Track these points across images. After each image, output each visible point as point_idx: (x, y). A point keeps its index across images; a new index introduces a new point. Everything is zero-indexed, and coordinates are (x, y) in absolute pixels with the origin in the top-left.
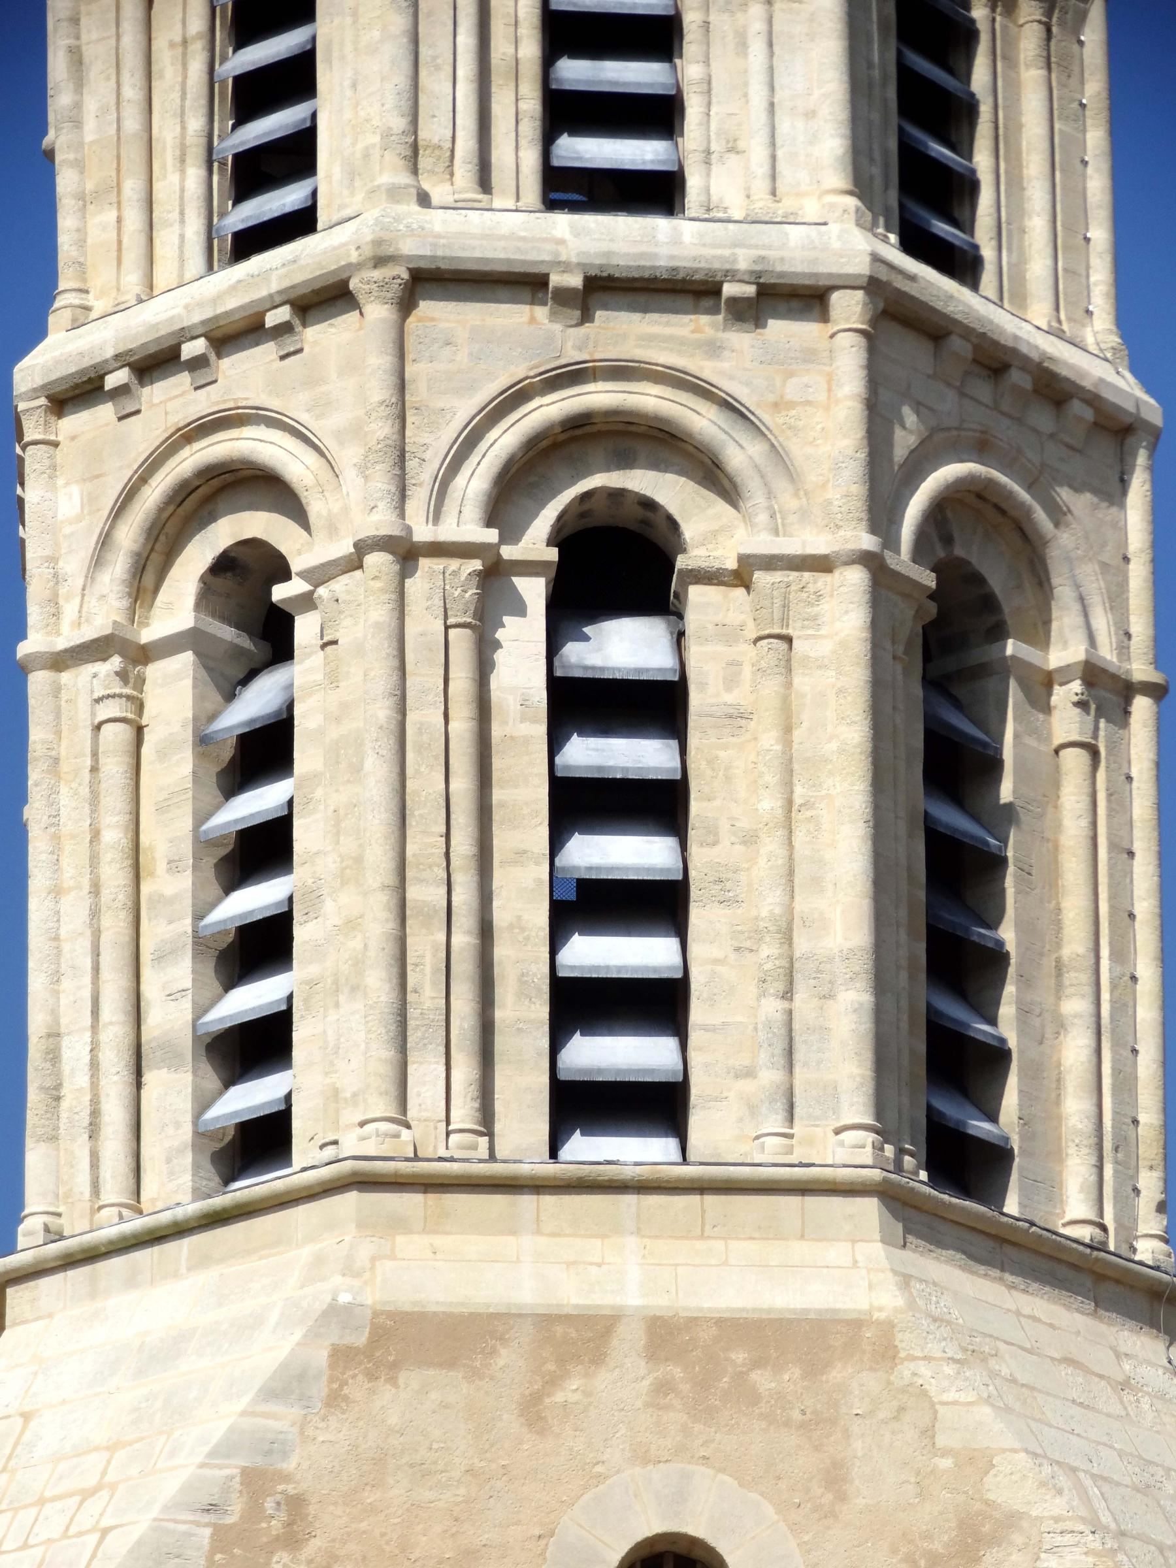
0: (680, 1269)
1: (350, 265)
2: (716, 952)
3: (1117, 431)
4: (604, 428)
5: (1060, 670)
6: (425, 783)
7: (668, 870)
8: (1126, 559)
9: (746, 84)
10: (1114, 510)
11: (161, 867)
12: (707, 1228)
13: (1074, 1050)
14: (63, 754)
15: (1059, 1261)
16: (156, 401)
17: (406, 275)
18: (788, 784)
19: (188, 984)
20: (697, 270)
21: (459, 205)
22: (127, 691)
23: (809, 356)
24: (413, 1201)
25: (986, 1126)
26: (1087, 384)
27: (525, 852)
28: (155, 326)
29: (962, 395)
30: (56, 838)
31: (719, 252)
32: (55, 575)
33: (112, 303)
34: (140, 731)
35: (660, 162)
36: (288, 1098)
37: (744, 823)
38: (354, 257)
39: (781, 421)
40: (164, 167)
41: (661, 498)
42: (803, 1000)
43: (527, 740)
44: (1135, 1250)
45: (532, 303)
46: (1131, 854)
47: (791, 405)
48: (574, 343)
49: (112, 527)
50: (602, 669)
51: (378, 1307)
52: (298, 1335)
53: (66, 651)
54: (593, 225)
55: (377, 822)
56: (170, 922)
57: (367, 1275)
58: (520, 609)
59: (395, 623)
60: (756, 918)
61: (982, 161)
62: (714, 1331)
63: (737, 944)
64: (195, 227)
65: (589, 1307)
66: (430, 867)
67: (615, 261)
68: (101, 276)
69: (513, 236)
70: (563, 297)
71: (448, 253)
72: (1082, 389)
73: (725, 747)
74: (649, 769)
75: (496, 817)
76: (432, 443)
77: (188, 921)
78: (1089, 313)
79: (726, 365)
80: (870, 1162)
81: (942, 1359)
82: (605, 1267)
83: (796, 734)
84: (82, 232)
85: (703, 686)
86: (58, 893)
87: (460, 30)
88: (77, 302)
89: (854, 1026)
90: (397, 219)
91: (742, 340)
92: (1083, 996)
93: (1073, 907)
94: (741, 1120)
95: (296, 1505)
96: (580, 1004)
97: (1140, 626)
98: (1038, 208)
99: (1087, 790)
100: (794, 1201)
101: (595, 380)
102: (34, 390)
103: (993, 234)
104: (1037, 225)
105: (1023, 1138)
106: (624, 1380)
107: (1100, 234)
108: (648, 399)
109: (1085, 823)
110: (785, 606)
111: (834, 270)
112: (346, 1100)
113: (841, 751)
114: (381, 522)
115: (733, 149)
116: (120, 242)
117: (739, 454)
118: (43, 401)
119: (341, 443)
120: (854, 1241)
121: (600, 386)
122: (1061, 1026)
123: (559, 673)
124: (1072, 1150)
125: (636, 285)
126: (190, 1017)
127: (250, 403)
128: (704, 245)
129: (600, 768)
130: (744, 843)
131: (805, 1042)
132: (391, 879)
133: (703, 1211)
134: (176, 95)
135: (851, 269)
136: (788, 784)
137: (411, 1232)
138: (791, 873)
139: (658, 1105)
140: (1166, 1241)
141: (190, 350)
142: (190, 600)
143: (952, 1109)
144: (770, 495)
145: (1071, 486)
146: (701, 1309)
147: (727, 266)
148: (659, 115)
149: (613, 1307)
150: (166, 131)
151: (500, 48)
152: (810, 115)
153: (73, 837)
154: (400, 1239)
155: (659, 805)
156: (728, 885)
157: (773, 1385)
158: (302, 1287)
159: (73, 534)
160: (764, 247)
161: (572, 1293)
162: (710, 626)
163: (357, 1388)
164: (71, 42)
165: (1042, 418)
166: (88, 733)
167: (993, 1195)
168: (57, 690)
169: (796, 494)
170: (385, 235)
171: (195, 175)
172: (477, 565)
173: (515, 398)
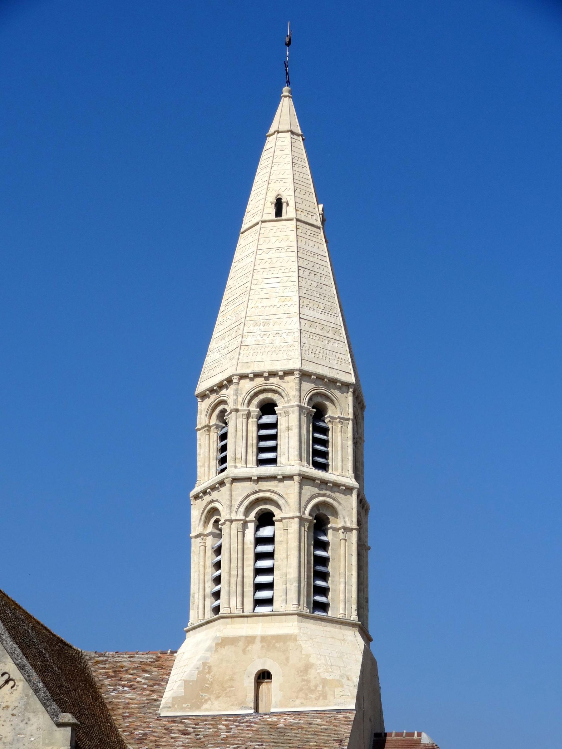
23: (291, 486)
42: (288, 586)
48: (256, 487)
64: (214, 470)
76: (236, 504)
91: (281, 484)
95: (210, 667)
104: (340, 457)
106: (257, 646)
108: (267, 495)
117: (281, 502)
139: (269, 602)
161: (250, 633)
168: (195, 541)
171: (215, 462)
173: (248, 496)
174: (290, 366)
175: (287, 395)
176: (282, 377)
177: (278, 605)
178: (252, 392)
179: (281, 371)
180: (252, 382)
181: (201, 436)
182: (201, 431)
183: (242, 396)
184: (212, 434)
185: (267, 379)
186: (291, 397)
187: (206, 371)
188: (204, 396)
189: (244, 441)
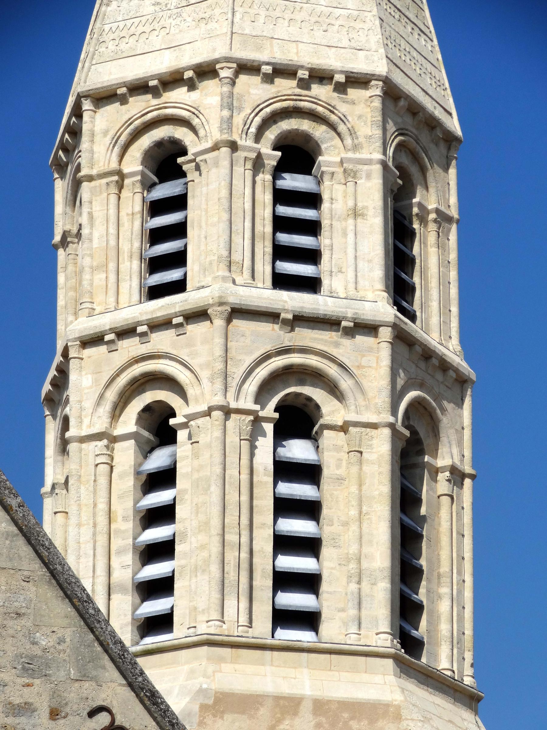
0: (323, 682)
1: (209, 304)
2: (332, 565)
3: (462, 382)
4: (295, 370)
5: (441, 467)
6: (232, 497)
7: (316, 534)
8: (463, 428)
9: (346, 248)
10: (460, 409)
11: (120, 519)
12: (332, 667)
13: (444, 606)
14: (82, 474)
15: (444, 684)
16: (124, 346)
17: (230, 310)
18: (360, 506)
19: (131, 563)
20: (333, 316)
21: (246, 285)
22: (109, 453)
23: (370, 350)
24: (227, 651)
25: (415, 632)
26: (455, 364)
27: (265, 524)
28: (127, 320)
29: (417, 366)
30: (79, 505)
31: (341, 310)
32: (81, 407)
33: (104, 308)
34: (112, 467)
35: (314, 274)
36: (172, 608)
37: (343, 518)
38: (211, 302)
39: (360, 373)
40: (124, 259)
41: (315, 397)
42: (365, 585)
43: (266, 483)
44: (463, 681)
45: (273, 323)
46: (463, 536)
47: (364, 367)
48: (288, 338)
49: (104, 392)
50: (293, 458)
51: (217, 690)
52: (188, 699)
53: (86, 436)
54: (296, 296)
55: (216, 510)
56: (123, 540)
57: (212, 678)
58: (264, 435)
59: (223, 438)
60: (347, 554)
61: (416, 279)
62: (337, 705)
63: (339, 563)
64: (135, 283)
65: (293, 694)
66: (233, 528)
67: (304, 310)
68: (99, 298)
69: (268, 298)
70: (285, 322)
71: (245, 303)
72: (453, 366)
73: (336, 490)
74: (309, 496)
75: (254, 511)
77: (131, 540)
78: (450, 337)
79: (341, 351)
80: (390, 646)
81: (418, 720)
82: (297, 679)
83: (364, 488)
84: (92, 280)
85: (329, 467)
86: (80, 526)
87: (246, 220)
88: (90, 306)
89: (384, 596)
90: (227, 289)
91: (347, 342)
92: (448, 587)
93: (444, 554)
94: (340, 627)
96: (283, 581)
97: (468, 453)
98: (435, 299)
99: (450, 512)
100: (363, 658)
101: (294, 353)
102: (75, 338)
103: (420, 307)
104: (434, 305)
105: (427, 638)
107: (455, 309)
108: (313, 361)
109: (449, 524)
110: (360, 440)
111: (382, 319)
112: (199, 612)
113: (380, 495)
114: (218, 400)
115: (340, 271)
116: (107, 286)
118: (78, 343)
119: (201, 369)
120: (384, 675)
121: (296, 355)
122: (440, 597)
123: (277, 459)
124: (443, 643)
125: (311, 319)
126: (131, 576)
127: (164, 351)
128: (336, 307)
129: (291, 495)
130: (342, 526)
131: (366, 600)
132: (220, 532)
133: (331, 661)
134: (130, 234)
135: (387, 320)
136: (360, 506)
137: (227, 663)
138: (361, 538)
139: (309, 620)
140: (473, 678)
141: (140, 329)
142: (134, 421)
143: (407, 627)
144: (355, 399)
145: (447, 401)
146: (332, 697)
147: (344, 315)
148: (312, 256)
149: (301, 695)
150: (125, 246)
151: (259, 228)
152: (370, 261)
153: (86, 505)
154: (223, 665)
155: (311, 509)
156: (337, 541)
157: (358, 726)
158: (187, 680)
159: (88, 393)
160: (357, 309)
161: (286, 688)
162: (331, 445)
163: (209, 720)
164: (89, 210)
165: (439, 376)
166: (93, 467)
167: (418, 657)
168: (81, 450)
169: (365, 400)
170: (223, 295)
171: (136, 263)
172: (251, 418)
173: (266, 357)
174: (360, 65)
175: (352, 132)
176: (341, 88)
177: (331, 630)
179: (342, 72)
180: (267, 86)
181: (93, 192)
182: (93, 183)
183: (243, 115)
184: (125, 193)
185: (304, 84)
186: (361, 140)
188: (104, 97)
189: (248, 224)
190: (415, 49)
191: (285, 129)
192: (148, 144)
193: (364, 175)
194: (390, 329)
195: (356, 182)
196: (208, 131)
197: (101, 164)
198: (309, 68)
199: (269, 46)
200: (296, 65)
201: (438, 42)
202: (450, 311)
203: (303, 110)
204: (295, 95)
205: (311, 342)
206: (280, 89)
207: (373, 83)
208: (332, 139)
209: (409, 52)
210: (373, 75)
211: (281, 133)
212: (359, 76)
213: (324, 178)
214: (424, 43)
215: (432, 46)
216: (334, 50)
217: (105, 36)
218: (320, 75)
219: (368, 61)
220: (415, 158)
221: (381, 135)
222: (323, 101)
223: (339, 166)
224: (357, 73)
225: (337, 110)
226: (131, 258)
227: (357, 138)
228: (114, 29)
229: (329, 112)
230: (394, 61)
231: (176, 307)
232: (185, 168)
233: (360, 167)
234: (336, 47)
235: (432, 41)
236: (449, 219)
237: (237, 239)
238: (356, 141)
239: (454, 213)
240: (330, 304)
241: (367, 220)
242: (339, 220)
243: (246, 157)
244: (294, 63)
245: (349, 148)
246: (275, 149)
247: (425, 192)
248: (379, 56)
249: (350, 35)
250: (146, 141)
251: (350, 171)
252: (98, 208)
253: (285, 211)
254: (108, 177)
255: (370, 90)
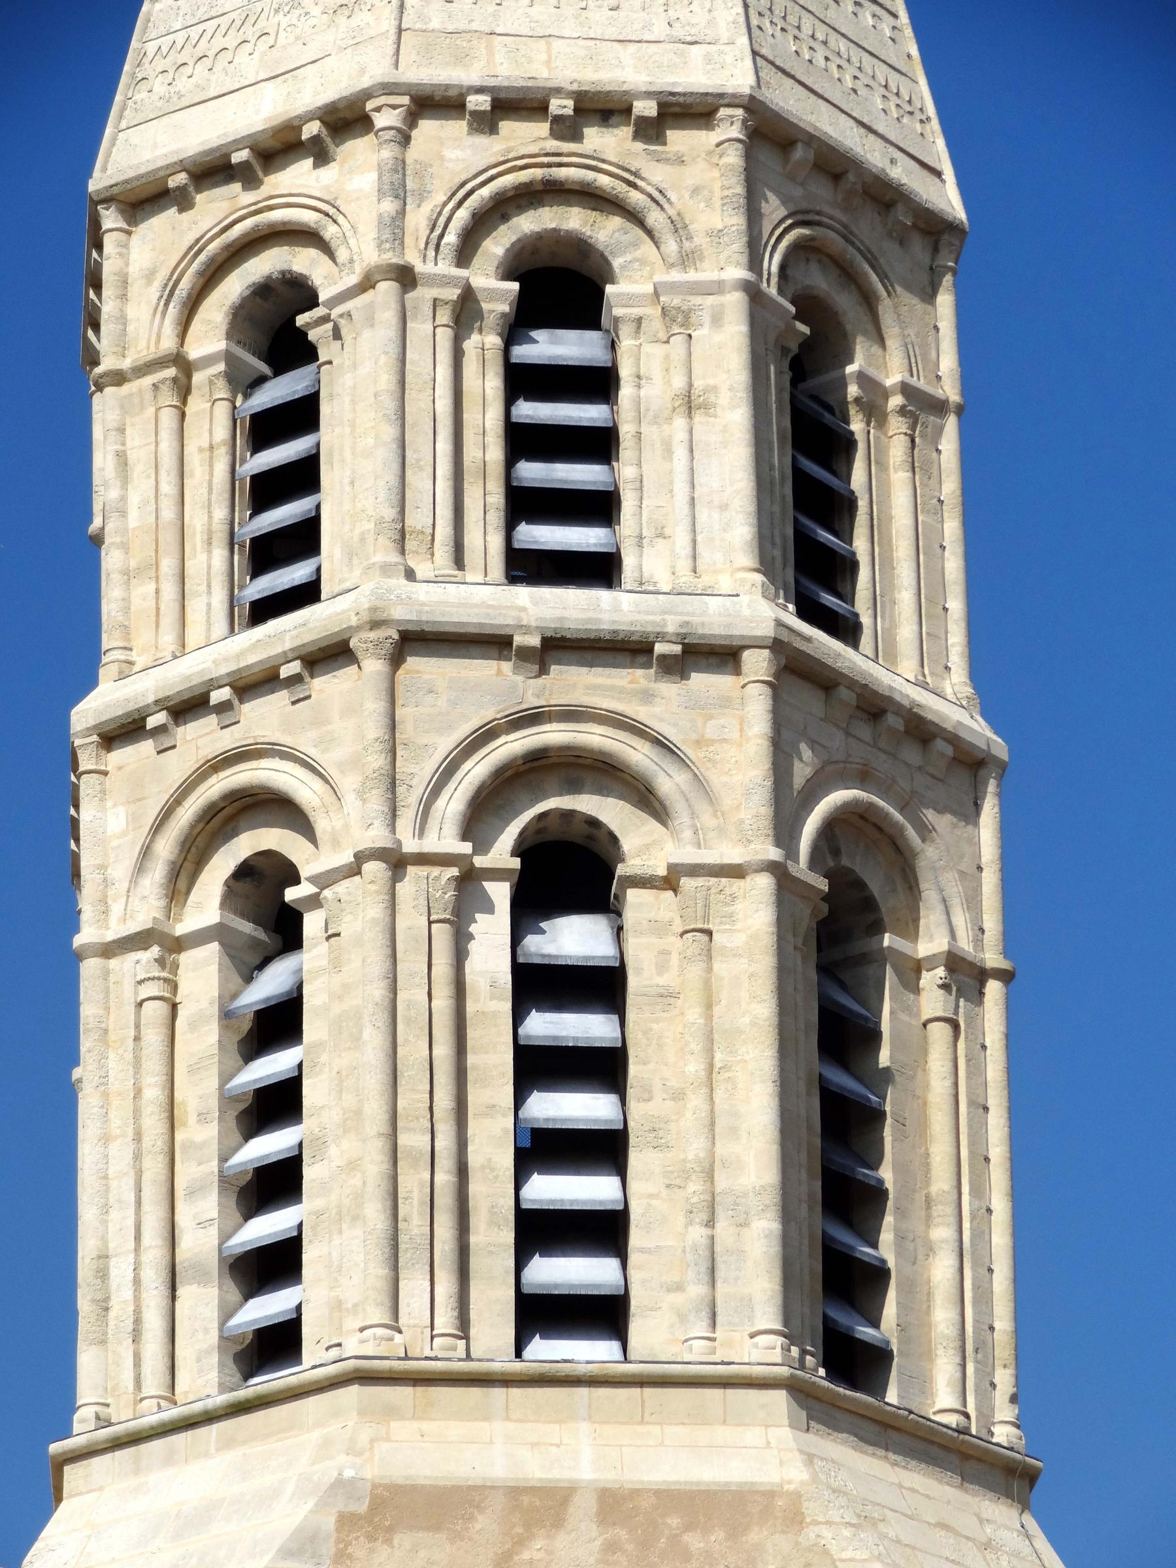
0: (624, 1449)
1: (350, 628)
2: (650, 1188)
3: (971, 764)
4: (556, 760)
5: (927, 958)
6: (413, 1050)
7: (611, 1121)
8: (980, 869)
9: (671, 482)
10: (970, 827)
11: (192, 1119)
12: (646, 1415)
13: (941, 1269)
14: (111, 1027)
15: (932, 1443)
16: (188, 738)
17: (396, 636)
18: (710, 1051)
19: (216, 1215)
20: (633, 633)
21: (439, 579)
22: (165, 974)
23: (725, 702)
24: (403, 1394)
25: (870, 1331)
26: (948, 726)
27: (494, 1106)
28: (188, 678)
29: (848, 734)
30: (106, 1095)
31: (651, 618)
32: (105, 880)
33: (151, 658)
34: (174, 1007)
35: (601, 545)
36: (299, 1308)
37: (673, 1083)
38: (354, 621)
39: (702, 755)
40: (194, 548)
41: (603, 818)
42: (723, 1228)
43: (495, 1015)
44: (992, 1434)
45: (499, 659)
46: (986, 1109)
47: (711, 742)
48: (533, 691)
49: (152, 841)
50: (557, 957)
51: (377, 1481)
52: (310, 1504)
53: (114, 941)
54: (548, 596)
55: (374, 1081)
56: (200, 1164)
57: (367, 1454)
58: (489, 908)
59: (388, 919)
60: (684, 1160)
61: (860, 545)
62: (653, 1500)
63: (667, 1182)
64: (219, 597)
65: (550, 1480)
66: (417, 1118)
68: (142, 638)
69: (484, 604)
70: (525, 654)
71: (431, 618)
73: (657, 1021)
74: (595, 1039)
75: (471, 1076)
76: (418, 772)
77: (215, 1163)
78: (947, 668)
79: (657, 710)
80: (779, 1361)
81: (842, 1523)
82: (562, 1447)
83: (717, 1010)
84: (126, 600)
85: (639, 971)
86: (107, 1140)
87: (438, 438)
88: (123, 658)
89: (765, 1249)
90: (390, 591)
91: (670, 690)
92: (948, 1225)
93: (940, 1151)
94: (672, 1326)
96: (539, 1231)
97: (992, 922)
99: (950, 1056)
100: (716, 1393)
101: (550, 722)
102: (88, 729)
103: (870, 604)
104: (905, 598)
105: (899, 1343)
107: (956, 605)
108: (594, 737)
109: (948, 1083)
110: (707, 906)
112: (348, 1309)
113: (753, 1024)
114: (376, 836)
115: (661, 535)
116: (158, 609)
117: (668, 782)
118: (95, 738)
119: (342, 772)
120: (767, 1426)
121: (555, 726)
122: (930, 1250)
123: (521, 960)
124: (940, 1352)
125: (583, 645)
126: (216, 1242)
129: (555, 1038)
130: (673, 1099)
131: (725, 1262)
132: (385, 1128)
133: (643, 1401)
134: (205, 491)
135: (759, 633)
136: (710, 1051)
137: (403, 1419)
138: (713, 1124)
139: (605, 1314)
140: (1018, 1427)
141: (217, 696)
142: (216, 901)
143: (843, 1317)
144: (693, 815)
145: (935, 809)
146: (642, 1482)
147: (658, 630)
148: (600, 507)
149: (569, 1481)
150: (196, 520)
151: (471, 453)
152: (724, 507)
153: (120, 1094)
154: (394, 1425)
155: (604, 1068)
156: (661, 1133)
157: (702, 1545)
158: (313, 1464)
159: (119, 847)
160: (688, 614)
161: (536, 1469)
162: (645, 923)
163: (359, 1549)
164: (119, 447)
165: (911, 754)
166: (132, 1009)
167: (879, 1390)
168: (106, 973)
169: (715, 815)
170: (379, 604)
171: (219, 555)
172: (454, 871)
173: (485, 735)
174: (692, 76)
175: (678, 226)
177: (654, 1333)
178: (485, 192)
179: (649, 95)
180: (482, 140)
181: (125, 408)
182: (126, 388)
183: (428, 208)
184: (196, 404)
185: (567, 129)
186: (700, 240)
187: (147, 70)
188: (146, 199)
189: (444, 446)
190: (843, 35)
191: (527, 231)
192: (239, 291)
193: (706, 318)
194: (766, 652)
195: (690, 336)
196: (355, 249)
197: (142, 344)
198: (573, 92)
199: (484, 52)
200: (544, 88)
201: (911, 17)
202: (945, 609)
203: (567, 187)
204: (547, 155)
205: (588, 694)
206: (512, 144)
207: (723, 112)
208: (636, 245)
209: (825, 43)
210: (721, 95)
211: (519, 240)
212: (689, 100)
213: (620, 333)
214: (870, 21)
215: (894, 28)
216: (632, 48)
217: (147, 65)
218: (600, 106)
219: (709, 67)
220: (849, 276)
221: (744, 227)
222: (611, 163)
223: (653, 304)
224: (684, 94)
225: (643, 179)
226: (210, 544)
227: (690, 238)
228: (164, 50)
229: (624, 185)
230: (777, 63)
231: (284, 642)
232: (312, 335)
233: (698, 300)
234: (639, 42)
235: (895, 16)
236: (939, 407)
237: (418, 482)
238: (687, 244)
239: (950, 391)
240: (625, 607)
241: (715, 416)
242: (655, 421)
243: (435, 300)
244: (541, 84)
245: (671, 261)
246: (508, 276)
247: (876, 349)
248: (737, 52)
249: (671, 12)
250: (235, 286)
251: (674, 312)
252: (137, 443)
253: (530, 411)
254: (156, 372)
255: (718, 130)
